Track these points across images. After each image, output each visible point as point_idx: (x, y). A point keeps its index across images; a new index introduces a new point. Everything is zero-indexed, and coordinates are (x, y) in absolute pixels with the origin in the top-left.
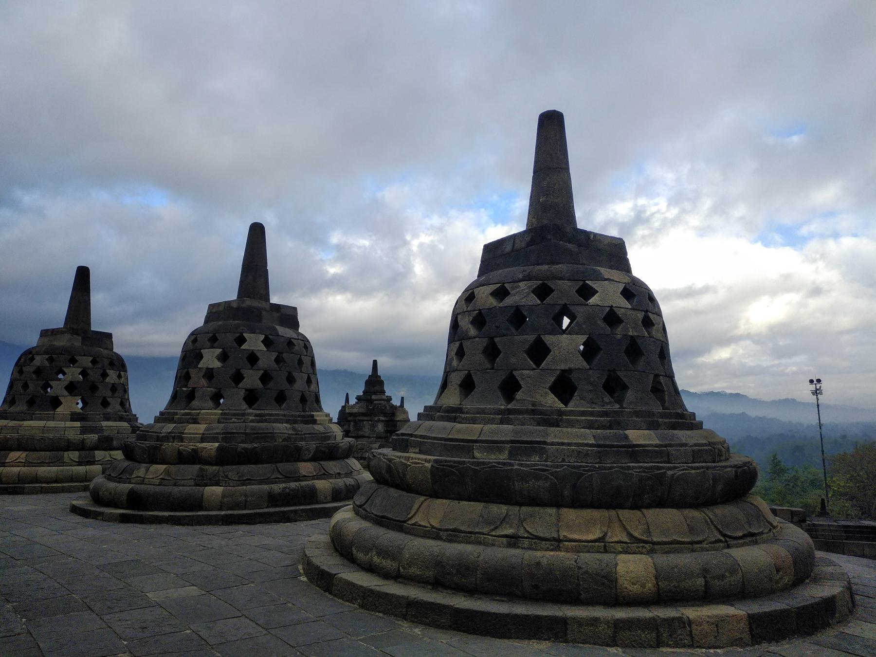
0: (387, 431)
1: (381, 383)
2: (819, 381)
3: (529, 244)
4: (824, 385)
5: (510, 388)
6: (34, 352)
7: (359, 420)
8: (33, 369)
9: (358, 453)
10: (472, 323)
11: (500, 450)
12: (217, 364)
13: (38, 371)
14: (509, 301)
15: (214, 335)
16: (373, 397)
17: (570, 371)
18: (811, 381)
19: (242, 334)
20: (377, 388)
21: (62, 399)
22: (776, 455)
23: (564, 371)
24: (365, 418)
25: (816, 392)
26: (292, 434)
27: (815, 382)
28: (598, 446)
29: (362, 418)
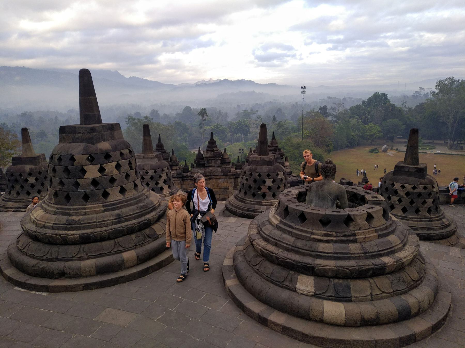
0: (221, 163)
1: (215, 142)
2: (305, 87)
3: (415, 172)
4: (306, 90)
5: (417, 211)
6: (146, 168)
7: (209, 160)
8: (149, 177)
9: (212, 173)
10: (405, 194)
11: (425, 229)
12: (272, 184)
13: (152, 178)
14: (416, 190)
15: (268, 173)
16: (214, 149)
17: (430, 207)
18: (302, 87)
19: (277, 172)
20: (215, 145)
21: (163, 187)
22: (275, 116)
23: (429, 208)
24: (212, 159)
25: (303, 92)
27: (303, 88)
28: (442, 226)
29: (210, 159)
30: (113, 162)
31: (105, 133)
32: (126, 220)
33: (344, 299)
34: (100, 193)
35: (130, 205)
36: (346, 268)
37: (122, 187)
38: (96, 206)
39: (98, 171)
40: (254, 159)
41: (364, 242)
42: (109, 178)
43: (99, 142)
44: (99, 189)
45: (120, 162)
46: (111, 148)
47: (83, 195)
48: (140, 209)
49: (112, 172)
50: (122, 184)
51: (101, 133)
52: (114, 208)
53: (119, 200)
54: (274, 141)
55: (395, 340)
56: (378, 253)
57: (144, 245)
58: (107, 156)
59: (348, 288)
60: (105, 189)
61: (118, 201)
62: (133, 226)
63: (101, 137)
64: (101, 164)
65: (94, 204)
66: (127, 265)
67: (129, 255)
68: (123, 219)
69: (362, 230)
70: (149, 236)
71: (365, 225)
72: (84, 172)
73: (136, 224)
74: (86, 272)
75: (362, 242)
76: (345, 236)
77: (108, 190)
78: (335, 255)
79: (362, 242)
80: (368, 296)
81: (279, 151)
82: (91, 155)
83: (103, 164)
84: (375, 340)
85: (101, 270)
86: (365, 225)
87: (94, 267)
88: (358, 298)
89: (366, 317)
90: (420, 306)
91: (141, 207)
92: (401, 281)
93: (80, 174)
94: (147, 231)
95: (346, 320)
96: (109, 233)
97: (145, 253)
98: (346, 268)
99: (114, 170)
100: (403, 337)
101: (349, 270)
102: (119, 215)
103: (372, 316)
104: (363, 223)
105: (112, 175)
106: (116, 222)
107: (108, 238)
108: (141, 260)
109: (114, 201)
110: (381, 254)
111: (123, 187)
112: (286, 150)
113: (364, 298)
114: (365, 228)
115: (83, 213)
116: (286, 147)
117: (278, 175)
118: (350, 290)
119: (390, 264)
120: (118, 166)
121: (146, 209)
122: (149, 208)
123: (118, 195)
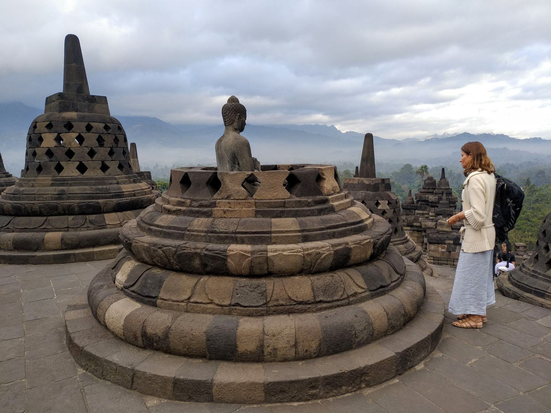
19: (377, 201)
22: (529, 178)
26: (406, 251)
30: (73, 132)
31: (79, 103)
32: (68, 198)
33: (147, 299)
34: (53, 165)
35: (86, 184)
36: (160, 248)
37: (81, 162)
38: (46, 179)
40: (351, 182)
41: (225, 217)
42: (66, 149)
43: (67, 112)
44: (52, 161)
45: (82, 134)
46: (76, 117)
47: (37, 166)
48: (95, 191)
49: (70, 143)
50: (81, 160)
51: (72, 101)
52: (63, 184)
53: (73, 176)
54: (442, 181)
55: (165, 380)
56: (233, 235)
57: (81, 230)
58: (69, 126)
59: (161, 282)
60: (59, 162)
61: (70, 177)
62: (71, 205)
63: (71, 106)
64: (59, 134)
65: (45, 177)
66: (47, 245)
67: (54, 237)
68: (64, 196)
69: (231, 200)
70: (92, 222)
71: (239, 192)
72: (41, 140)
73: (76, 204)
74: (3, 244)
75: (221, 217)
76: (201, 206)
77: (62, 163)
78: (166, 230)
79: (221, 217)
80: (182, 301)
81: (446, 196)
82: (52, 122)
83: (61, 133)
84: (133, 370)
85: (19, 245)
86: (239, 192)
87: (11, 240)
88: (167, 302)
89: (150, 330)
90: (263, 340)
91: (98, 189)
92: (258, 291)
93: (38, 142)
94: (93, 217)
95: (123, 329)
96: (40, 207)
97: (74, 237)
98: (160, 248)
100: (183, 381)
101: (162, 251)
102: (63, 191)
103: (157, 332)
104: (236, 188)
105: (69, 146)
106: (56, 197)
107: (40, 214)
108: (66, 245)
109: (65, 176)
110: (236, 238)
111: (83, 164)
112: (531, 223)
113: (175, 303)
114: (236, 198)
115: (31, 185)
116: (532, 219)
117: (378, 204)
118: (160, 287)
119: (234, 253)
120: (80, 139)
121: (103, 192)
122: (110, 193)
123: (74, 171)
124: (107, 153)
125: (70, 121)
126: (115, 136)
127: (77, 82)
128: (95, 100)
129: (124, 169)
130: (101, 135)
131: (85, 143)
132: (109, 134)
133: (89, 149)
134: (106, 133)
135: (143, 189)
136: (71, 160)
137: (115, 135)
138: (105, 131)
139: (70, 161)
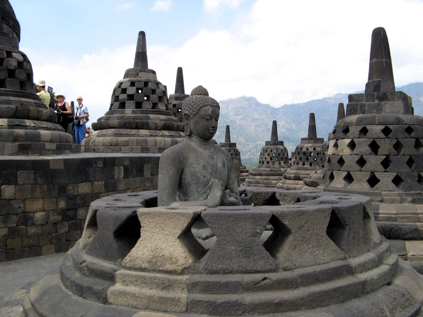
31: (367, 103)
37: (349, 172)
39: (334, 146)
42: (339, 157)
43: (354, 115)
49: (342, 150)
51: (361, 102)
63: (359, 108)
99: (345, 149)
105: (342, 154)
120: (352, 145)
124: (379, 162)
125: (348, 125)
126: (398, 141)
127: (375, 80)
128: (387, 97)
129: (404, 183)
130: (376, 140)
131: (356, 151)
132: (389, 138)
133: (358, 157)
134: (382, 137)
135: (417, 214)
136: (342, 169)
137: (397, 139)
138: (383, 136)
139: (340, 170)
